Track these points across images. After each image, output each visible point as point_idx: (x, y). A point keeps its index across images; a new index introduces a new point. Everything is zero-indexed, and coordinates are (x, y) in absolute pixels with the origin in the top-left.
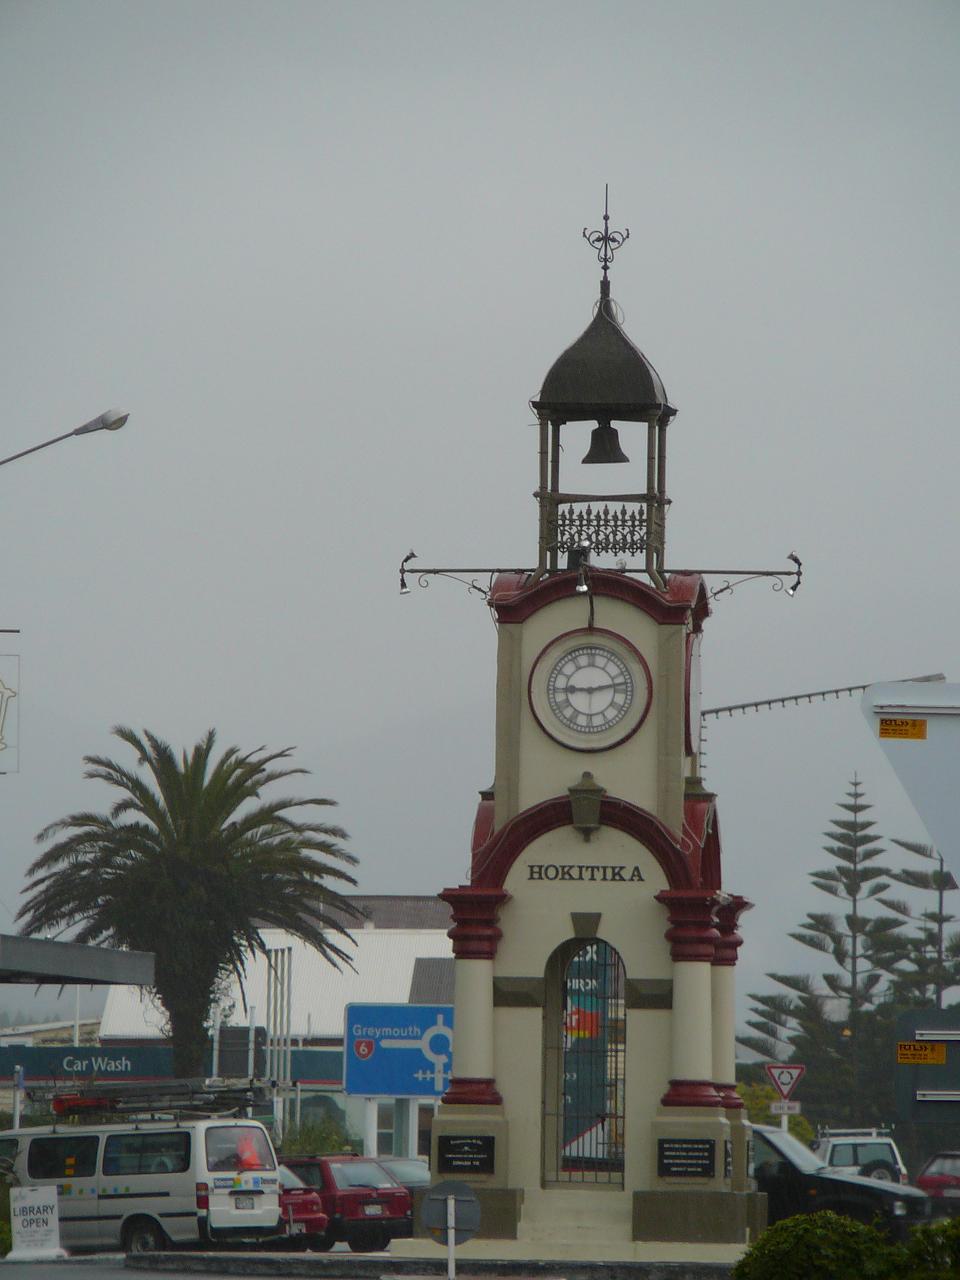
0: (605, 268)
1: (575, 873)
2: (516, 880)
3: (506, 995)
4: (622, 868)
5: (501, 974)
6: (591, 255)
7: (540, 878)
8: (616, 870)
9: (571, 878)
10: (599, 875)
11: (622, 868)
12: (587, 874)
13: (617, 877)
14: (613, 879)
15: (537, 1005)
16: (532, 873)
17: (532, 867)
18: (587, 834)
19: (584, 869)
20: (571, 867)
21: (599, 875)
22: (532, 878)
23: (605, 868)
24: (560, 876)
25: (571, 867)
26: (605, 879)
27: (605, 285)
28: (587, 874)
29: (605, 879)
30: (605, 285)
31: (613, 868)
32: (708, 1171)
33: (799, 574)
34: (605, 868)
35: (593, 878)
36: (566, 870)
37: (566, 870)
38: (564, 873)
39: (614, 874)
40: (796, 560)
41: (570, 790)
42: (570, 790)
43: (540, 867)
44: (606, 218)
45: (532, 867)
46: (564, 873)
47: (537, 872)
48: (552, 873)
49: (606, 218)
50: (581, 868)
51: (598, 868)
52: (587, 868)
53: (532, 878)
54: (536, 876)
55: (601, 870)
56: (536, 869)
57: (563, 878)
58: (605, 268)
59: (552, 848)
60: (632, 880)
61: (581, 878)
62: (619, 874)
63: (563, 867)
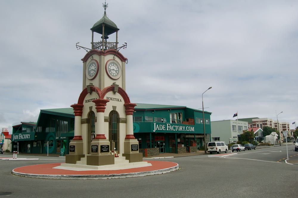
0: (105, 10)
1: (90, 101)
2: (84, 103)
3: (82, 122)
5: (82, 118)
6: (104, 8)
15: (85, 123)
18: (91, 94)
27: (105, 13)
30: (105, 13)
32: (108, 151)
33: (126, 45)
38: (89, 101)
40: (126, 43)
44: (105, 3)
47: (86, 102)
49: (105, 3)
58: (105, 10)
59: (88, 97)
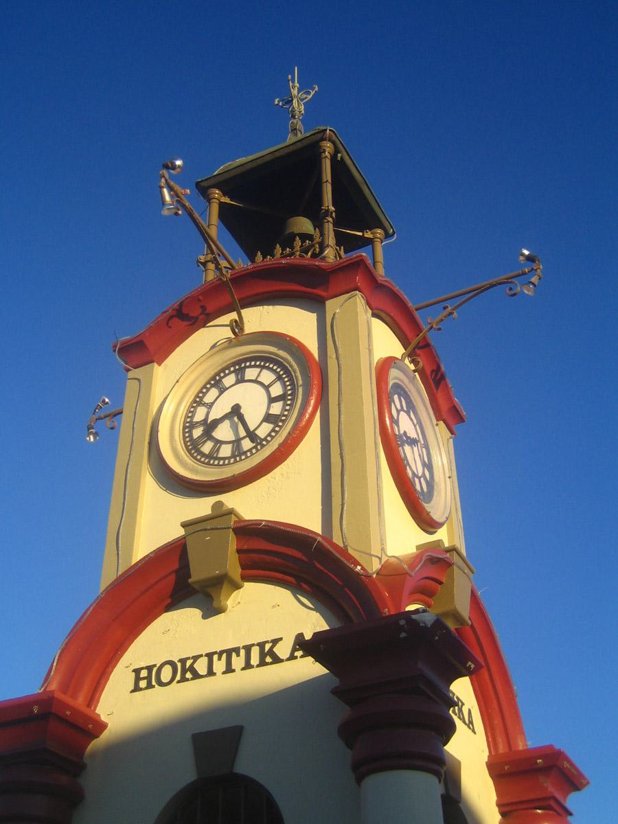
4: (275, 642)
7: (150, 686)
8: (267, 647)
9: (196, 676)
10: (238, 662)
11: (275, 642)
12: (219, 666)
13: (268, 659)
14: (262, 663)
16: (138, 679)
17: (137, 671)
19: (215, 657)
20: (196, 658)
21: (238, 662)
22: (137, 689)
23: (248, 649)
24: (178, 677)
25: (196, 658)
26: (248, 666)
28: (219, 666)
29: (248, 666)
31: (261, 645)
34: (248, 649)
35: (229, 669)
36: (189, 663)
37: (189, 663)
39: (263, 655)
41: (184, 525)
42: (184, 525)
43: (150, 668)
45: (137, 671)
46: (184, 671)
48: (166, 674)
50: (210, 656)
51: (237, 650)
52: (220, 654)
53: (137, 689)
54: (143, 684)
55: (242, 652)
56: (144, 673)
57: (183, 679)
60: (292, 657)
61: (211, 673)
62: (271, 653)
63: (183, 661)
